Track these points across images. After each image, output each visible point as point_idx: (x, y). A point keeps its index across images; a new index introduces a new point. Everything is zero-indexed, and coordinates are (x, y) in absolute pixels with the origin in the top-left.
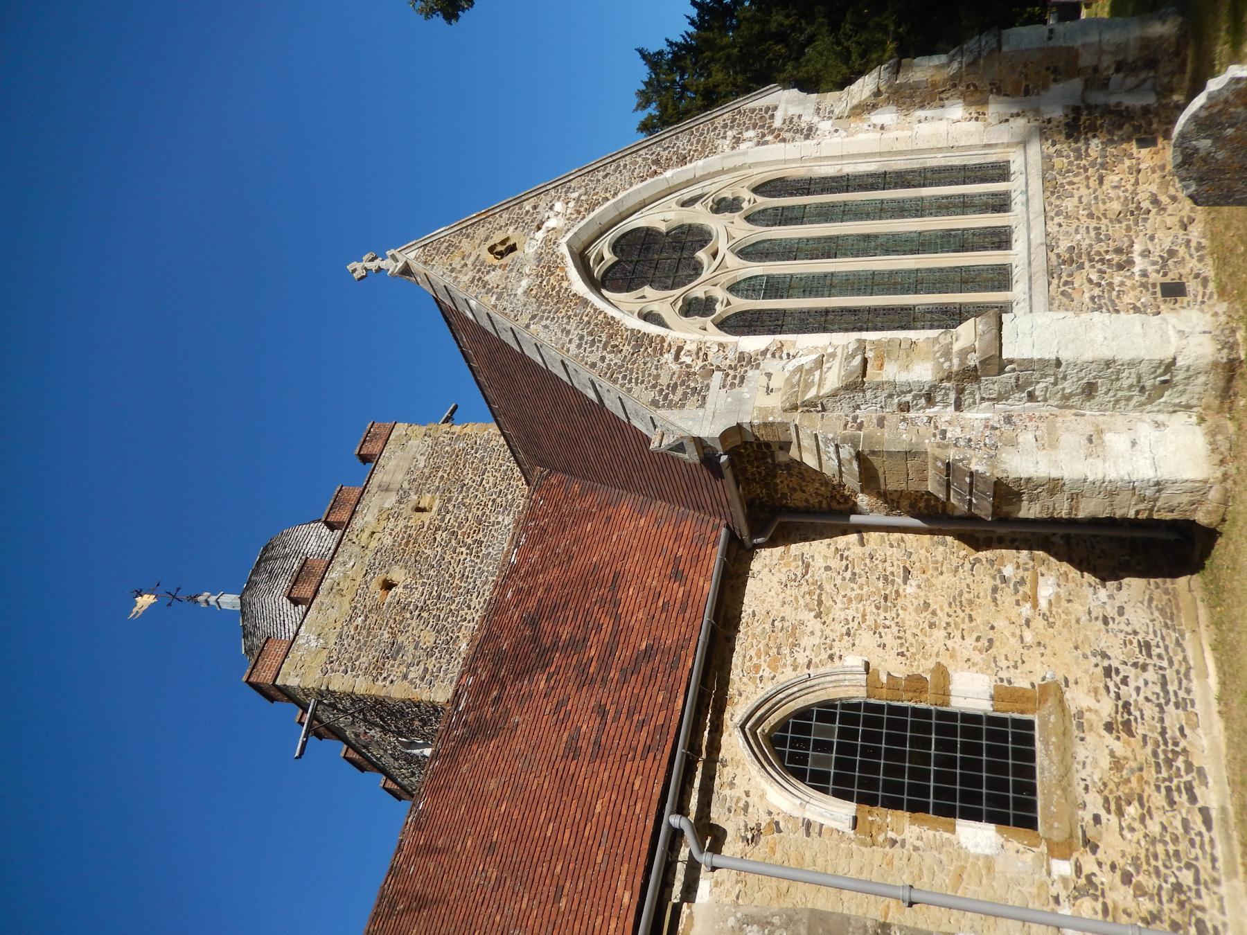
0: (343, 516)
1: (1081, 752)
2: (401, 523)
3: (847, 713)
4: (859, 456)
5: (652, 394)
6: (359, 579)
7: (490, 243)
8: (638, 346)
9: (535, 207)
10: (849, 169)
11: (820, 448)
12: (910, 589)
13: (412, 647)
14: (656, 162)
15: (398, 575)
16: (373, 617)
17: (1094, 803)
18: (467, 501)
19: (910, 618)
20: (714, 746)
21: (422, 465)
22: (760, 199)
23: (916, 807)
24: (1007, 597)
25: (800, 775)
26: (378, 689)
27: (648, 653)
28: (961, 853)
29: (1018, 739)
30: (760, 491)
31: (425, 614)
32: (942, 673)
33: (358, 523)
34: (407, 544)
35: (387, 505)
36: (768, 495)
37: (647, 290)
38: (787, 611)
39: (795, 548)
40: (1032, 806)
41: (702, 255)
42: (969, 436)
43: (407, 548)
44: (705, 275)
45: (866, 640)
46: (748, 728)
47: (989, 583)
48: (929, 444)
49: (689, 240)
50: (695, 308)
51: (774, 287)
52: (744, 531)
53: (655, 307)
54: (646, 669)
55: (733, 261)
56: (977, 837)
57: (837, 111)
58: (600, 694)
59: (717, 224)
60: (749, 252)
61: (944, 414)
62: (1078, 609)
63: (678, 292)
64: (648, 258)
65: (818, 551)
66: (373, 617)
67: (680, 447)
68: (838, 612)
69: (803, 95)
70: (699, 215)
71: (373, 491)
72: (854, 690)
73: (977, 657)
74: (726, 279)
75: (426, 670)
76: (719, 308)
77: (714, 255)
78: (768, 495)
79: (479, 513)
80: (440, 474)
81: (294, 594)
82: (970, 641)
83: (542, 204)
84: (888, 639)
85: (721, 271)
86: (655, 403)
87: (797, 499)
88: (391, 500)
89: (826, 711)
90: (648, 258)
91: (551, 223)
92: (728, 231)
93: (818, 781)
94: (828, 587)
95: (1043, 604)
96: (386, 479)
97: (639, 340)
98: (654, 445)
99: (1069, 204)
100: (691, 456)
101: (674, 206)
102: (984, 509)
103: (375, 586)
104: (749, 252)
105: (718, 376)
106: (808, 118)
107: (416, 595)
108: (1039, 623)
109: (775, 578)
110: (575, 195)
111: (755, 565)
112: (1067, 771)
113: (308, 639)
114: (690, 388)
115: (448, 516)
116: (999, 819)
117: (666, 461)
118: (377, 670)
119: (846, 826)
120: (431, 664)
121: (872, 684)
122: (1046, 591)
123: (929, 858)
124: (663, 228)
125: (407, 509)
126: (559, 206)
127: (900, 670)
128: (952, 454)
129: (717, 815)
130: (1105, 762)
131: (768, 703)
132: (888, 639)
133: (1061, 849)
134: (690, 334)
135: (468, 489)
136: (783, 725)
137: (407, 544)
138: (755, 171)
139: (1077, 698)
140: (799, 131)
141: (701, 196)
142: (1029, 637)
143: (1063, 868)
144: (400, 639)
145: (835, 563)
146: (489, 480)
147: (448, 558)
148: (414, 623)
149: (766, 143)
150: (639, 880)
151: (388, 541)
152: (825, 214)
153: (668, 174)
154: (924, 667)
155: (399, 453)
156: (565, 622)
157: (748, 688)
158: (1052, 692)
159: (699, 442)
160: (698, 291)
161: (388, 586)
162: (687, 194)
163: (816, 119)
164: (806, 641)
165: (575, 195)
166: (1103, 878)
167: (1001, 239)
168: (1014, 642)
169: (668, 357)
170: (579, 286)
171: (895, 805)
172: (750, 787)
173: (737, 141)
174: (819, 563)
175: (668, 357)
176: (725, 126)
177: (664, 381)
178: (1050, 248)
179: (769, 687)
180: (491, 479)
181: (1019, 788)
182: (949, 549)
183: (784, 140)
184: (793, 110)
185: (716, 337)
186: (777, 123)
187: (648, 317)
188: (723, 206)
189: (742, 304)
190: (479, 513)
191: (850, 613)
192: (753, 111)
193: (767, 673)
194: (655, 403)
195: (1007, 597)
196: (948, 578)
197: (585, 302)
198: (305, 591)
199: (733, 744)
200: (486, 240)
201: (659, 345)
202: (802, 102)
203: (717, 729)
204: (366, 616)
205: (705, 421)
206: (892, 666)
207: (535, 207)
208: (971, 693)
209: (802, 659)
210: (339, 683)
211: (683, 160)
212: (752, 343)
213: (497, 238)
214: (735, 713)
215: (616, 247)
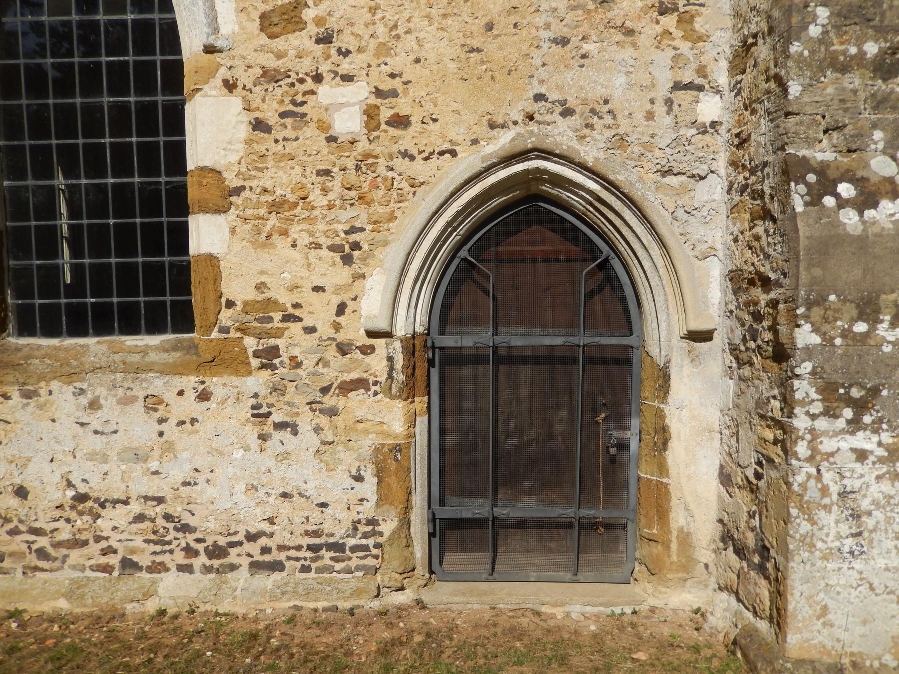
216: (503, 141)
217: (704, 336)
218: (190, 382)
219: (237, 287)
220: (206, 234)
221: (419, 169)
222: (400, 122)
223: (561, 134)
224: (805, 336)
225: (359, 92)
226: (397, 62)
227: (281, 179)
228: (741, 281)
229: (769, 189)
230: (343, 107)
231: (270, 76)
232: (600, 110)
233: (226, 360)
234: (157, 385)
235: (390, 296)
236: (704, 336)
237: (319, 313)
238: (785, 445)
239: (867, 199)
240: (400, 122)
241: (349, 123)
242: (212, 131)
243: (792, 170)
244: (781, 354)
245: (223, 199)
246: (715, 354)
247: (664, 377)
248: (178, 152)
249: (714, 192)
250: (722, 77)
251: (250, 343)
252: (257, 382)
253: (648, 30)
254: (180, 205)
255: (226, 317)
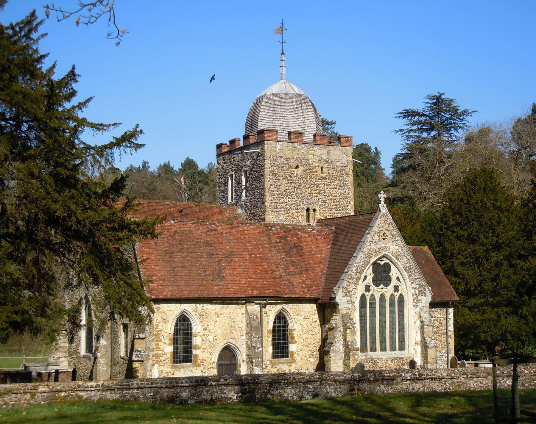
0: (318, 142)
1: (285, 365)
2: (317, 164)
3: (286, 326)
4: (333, 328)
5: (345, 286)
6: (298, 156)
7: (387, 232)
8: (356, 279)
9: (397, 241)
10: (405, 316)
11: (336, 320)
12: (310, 335)
13: (280, 184)
14: (410, 269)
15: (301, 169)
16: (287, 166)
17: (278, 367)
18: (326, 186)
19: (305, 336)
20: (279, 303)
21: (337, 164)
22: (397, 297)
23: (273, 339)
24: (310, 353)
25: (275, 319)
26: (267, 177)
27: (293, 285)
28: (268, 347)
29: (286, 356)
30: (328, 305)
31: (289, 184)
32: (295, 342)
33: (316, 148)
34: (311, 169)
35: (323, 156)
36: (327, 308)
37: (372, 275)
38: (304, 312)
39: (316, 311)
40: (276, 358)
41: (382, 286)
42: (338, 346)
43: (309, 169)
44: (376, 288)
45: (300, 328)
46: (283, 309)
47: (312, 350)
48: (336, 340)
49: (387, 281)
50: (367, 288)
51: (372, 304)
52: (320, 301)
53: (368, 278)
54: (290, 286)
55: (380, 294)
56: (270, 350)
57: (421, 312)
58: (283, 274)
59: (391, 287)
60: (382, 296)
61: (342, 342)
62: (309, 365)
63: (371, 283)
64: (382, 273)
65: (316, 317)
66: (287, 166)
67: (334, 294)
68: (305, 322)
69: (429, 302)
70: (394, 282)
71: (327, 149)
72: (290, 327)
73: (299, 348)
74: (374, 293)
75: (274, 191)
76: (366, 294)
77: (382, 289)
78: (327, 308)
79: (322, 192)
80: (334, 172)
81: (292, 135)
82: (301, 347)
83: (398, 242)
84: (300, 332)
85: (377, 291)
86: (343, 287)
87: (326, 312)
88: (325, 157)
89: (286, 322)
90: (382, 273)
91: (392, 247)
92: (388, 291)
93: (275, 322)
94: (309, 320)
95: (309, 359)
96: (332, 152)
97: (358, 280)
98: (334, 288)
99: (390, 362)
100: (333, 296)
101: (397, 276)
102: (326, 349)
103: (297, 163)
104: (382, 296)
105: (349, 298)
106: (420, 305)
107: (294, 179)
108: (306, 359)
109: (310, 310)
110: (400, 250)
111: (312, 305)
112: (282, 363)
113: (279, 146)
114: (347, 293)
115: (320, 181)
116: (273, 354)
117: (332, 291)
118: (272, 174)
119: (269, 329)
120: (276, 192)
121: (292, 330)
122: (312, 360)
123: (267, 342)
124: (390, 274)
125: (321, 165)
126: (397, 247)
127: (295, 335)
128: (334, 344)
129: (268, 306)
130: (284, 369)
131: (287, 312)
132: (300, 332)
133: (271, 362)
134: (360, 289)
135: (329, 185)
136: (283, 314)
137: (311, 169)
138: (406, 293)
139: (294, 365)
140: (416, 303)
141: (400, 282)
142: (303, 357)
143: (268, 363)
144: (281, 179)
145: (314, 320)
146: (333, 191)
147: (307, 186)
148: (286, 182)
149: (413, 296)
150: (258, 296)
151: (311, 162)
152: (392, 313)
153: (405, 273)
154: (296, 339)
155: (341, 153)
156: (296, 257)
157: (289, 307)
158: (294, 361)
159: (335, 298)
160: (373, 287)
161: (297, 167)
162: (401, 278)
163: (420, 307)
164: (298, 317)
165: (400, 250)
166: (268, 368)
167: (383, 349)
168: (302, 355)
169: (354, 287)
170: (372, 261)
171: (273, 336)
172: (272, 311)
173: (415, 289)
174: (314, 317)
175: (354, 287)
176: (420, 284)
177: (348, 287)
178: (378, 359)
179: (290, 312)
180: (333, 192)
181: (281, 356)
182: (319, 343)
183: (414, 300)
184: (424, 301)
185: (359, 296)
186: (419, 298)
187: (365, 277)
188: (396, 288)
189: (368, 299)
190: (322, 192)
191: (304, 325)
192: (425, 290)
193: (292, 310)
194: (343, 287)
195: (310, 353)
196: (313, 342)
197: (368, 264)
198: (293, 138)
199: (279, 307)
200: (388, 231)
201: (356, 285)
202: (426, 302)
203: (281, 303)
204: (286, 164)
205: (340, 298)
206: (295, 334)
207: (397, 241)
208: (292, 348)
209: (295, 317)
210: (267, 163)
211: (410, 276)
212: (357, 304)
213: (387, 233)
214: (285, 306)
215: (386, 263)
216: (226, 341)
217: (243, 361)
218: (195, 368)
219: (200, 357)
220: (194, 352)
221: (218, 344)
222: (216, 340)
223: (231, 341)
224: (254, 360)
225: (212, 337)
226: (216, 333)
227: (205, 346)
228: (247, 355)
229: (250, 347)
230: (211, 338)
231: (204, 335)
232: (234, 338)
233: (199, 366)
234: (192, 368)
235: (215, 358)
236: (243, 361)
237: (208, 360)
238: (253, 370)
239: (258, 349)
240: (216, 340)
241: (211, 340)
242: (196, 341)
243: (252, 346)
244: (252, 362)
245: (197, 347)
246: (245, 362)
247: (240, 365)
248: (191, 342)
249: (244, 346)
250: (245, 334)
251: (201, 364)
252: (202, 368)
253: (238, 330)
254: (191, 348)
255: (199, 361)
